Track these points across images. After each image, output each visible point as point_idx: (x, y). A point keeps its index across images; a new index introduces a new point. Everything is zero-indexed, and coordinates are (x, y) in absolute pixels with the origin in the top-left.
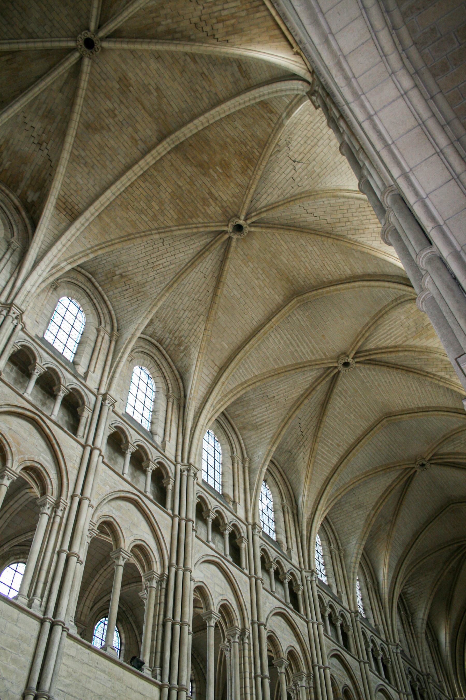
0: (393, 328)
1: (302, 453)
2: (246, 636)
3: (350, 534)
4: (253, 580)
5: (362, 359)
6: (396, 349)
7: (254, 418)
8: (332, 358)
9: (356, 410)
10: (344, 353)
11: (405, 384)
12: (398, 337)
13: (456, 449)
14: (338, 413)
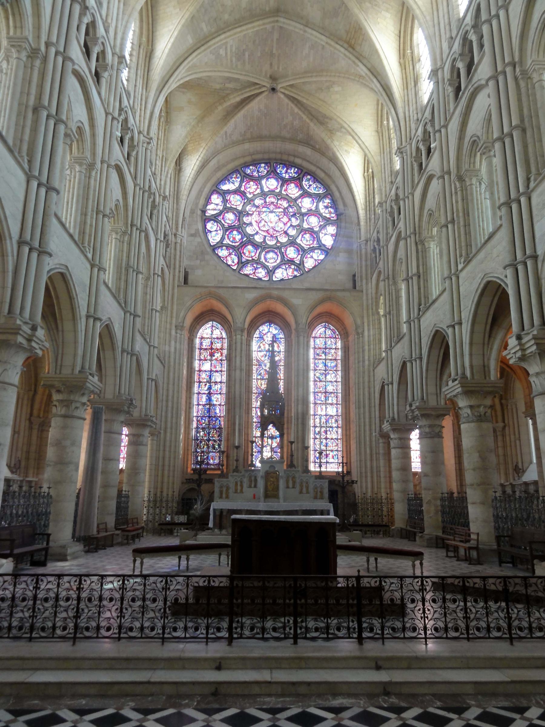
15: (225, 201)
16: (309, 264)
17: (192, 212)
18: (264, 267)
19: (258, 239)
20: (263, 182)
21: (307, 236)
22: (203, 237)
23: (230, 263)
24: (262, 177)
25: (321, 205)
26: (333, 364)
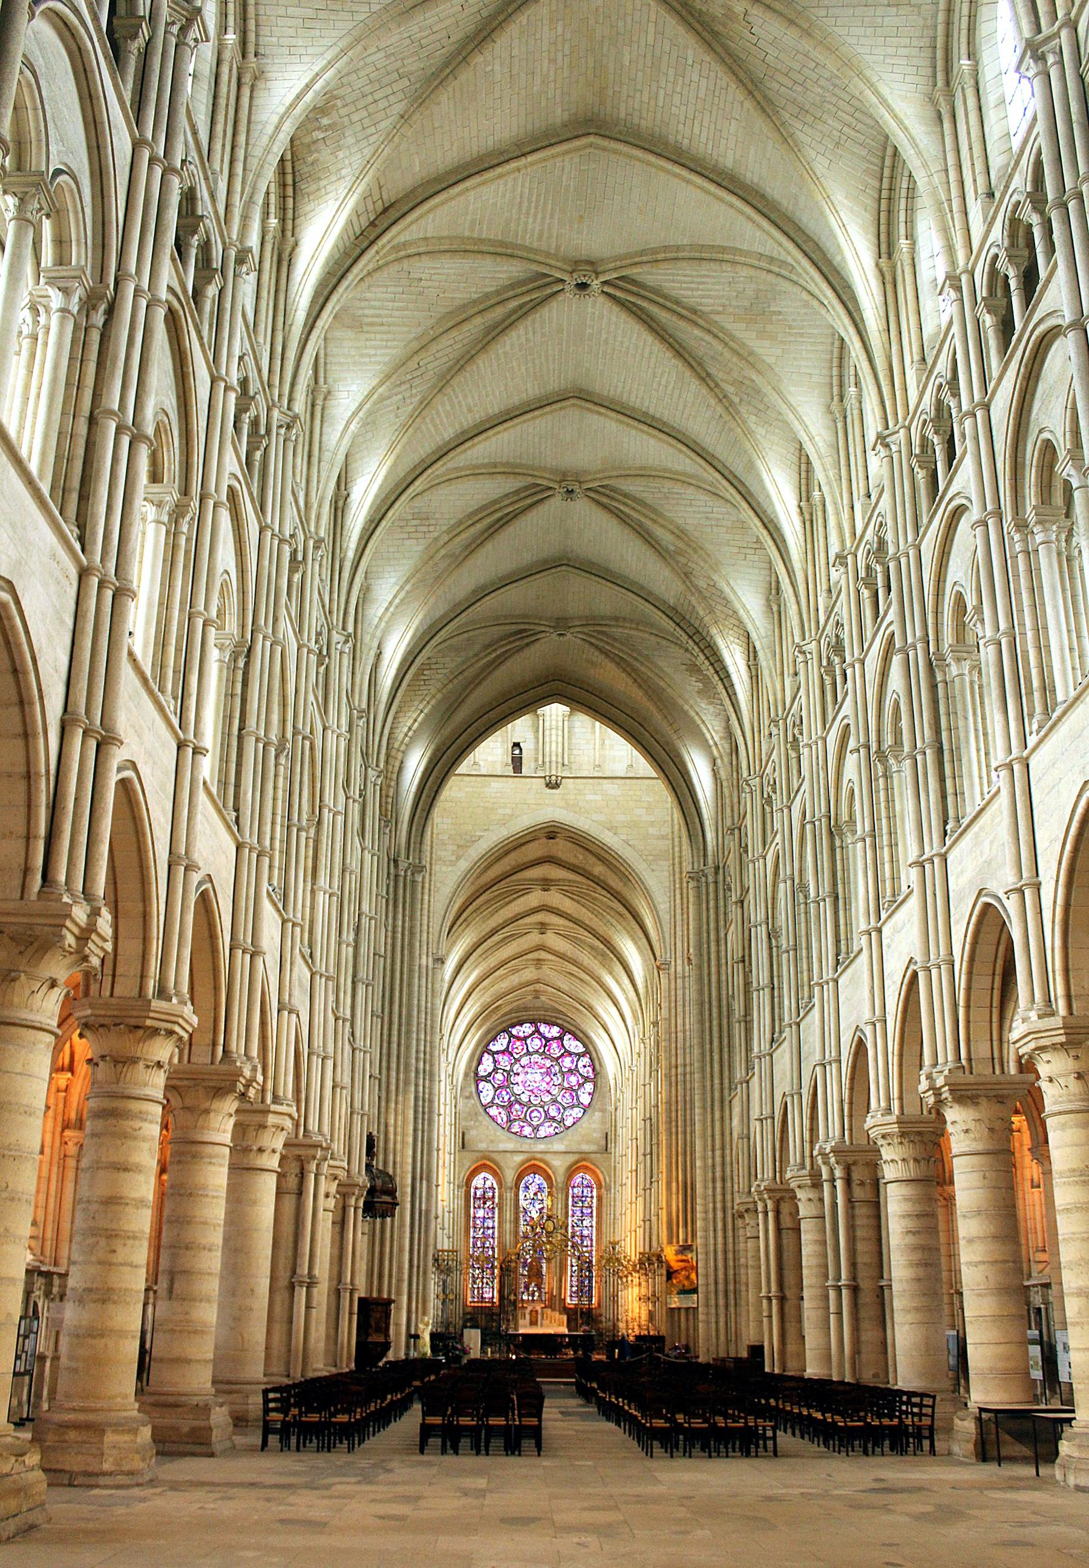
0: (713, 277)
1: (400, 396)
2: (285, 753)
3: (389, 559)
4: (306, 650)
5: (619, 294)
6: (694, 317)
7: (363, 304)
8: (564, 260)
9: (537, 362)
10: (591, 263)
11: (652, 365)
12: (709, 297)
13: (644, 495)
14: (505, 354)
15: (495, 1061)
16: (569, 1122)
17: (466, 1075)
18: (530, 1125)
19: (524, 1098)
20: (529, 1041)
21: (567, 1095)
22: (476, 1098)
23: (499, 1121)
24: (528, 1037)
25: (580, 1064)
26: (589, 1211)
